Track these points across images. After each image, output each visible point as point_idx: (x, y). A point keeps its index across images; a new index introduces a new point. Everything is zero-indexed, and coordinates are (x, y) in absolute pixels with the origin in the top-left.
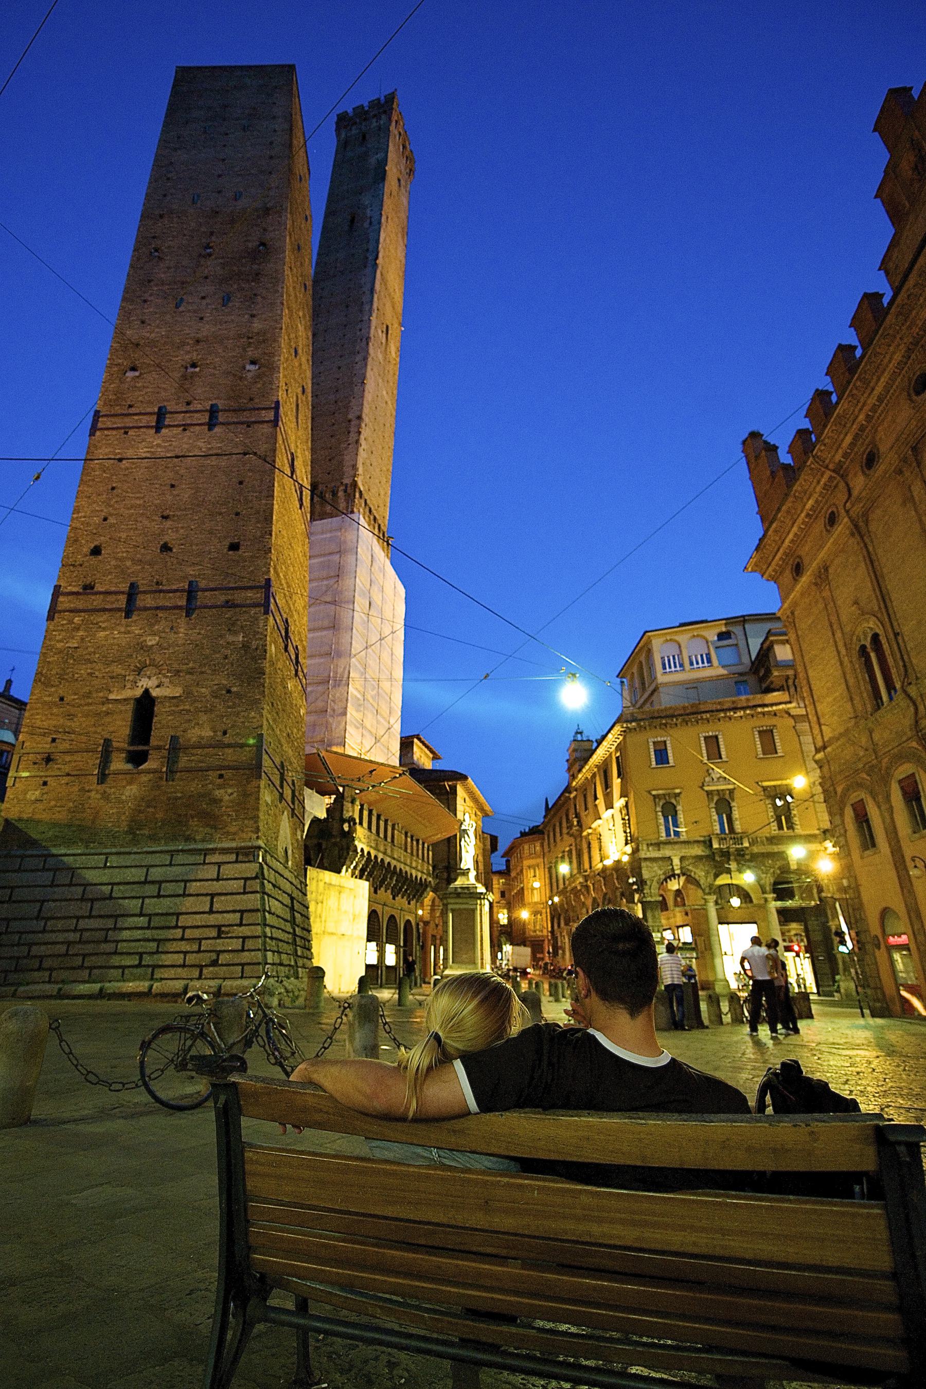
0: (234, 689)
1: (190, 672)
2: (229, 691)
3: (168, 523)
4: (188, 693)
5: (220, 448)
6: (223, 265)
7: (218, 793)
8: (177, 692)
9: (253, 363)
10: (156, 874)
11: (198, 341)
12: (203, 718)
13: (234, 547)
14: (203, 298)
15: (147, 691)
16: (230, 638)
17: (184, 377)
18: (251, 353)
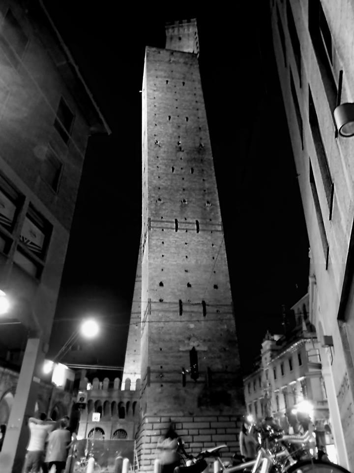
0: (227, 349)
1: (209, 341)
2: (225, 349)
3: (188, 274)
4: (209, 348)
5: (202, 241)
6: (188, 153)
7: (229, 392)
8: (205, 349)
9: (208, 202)
10: (213, 425)
11: (184, 190)
12: (218, 360)
13: (216, 287)
14: (182, 169)
15: (194, 348)
16: (222, 327)
17: (182, 206)
18: (207, 198)
